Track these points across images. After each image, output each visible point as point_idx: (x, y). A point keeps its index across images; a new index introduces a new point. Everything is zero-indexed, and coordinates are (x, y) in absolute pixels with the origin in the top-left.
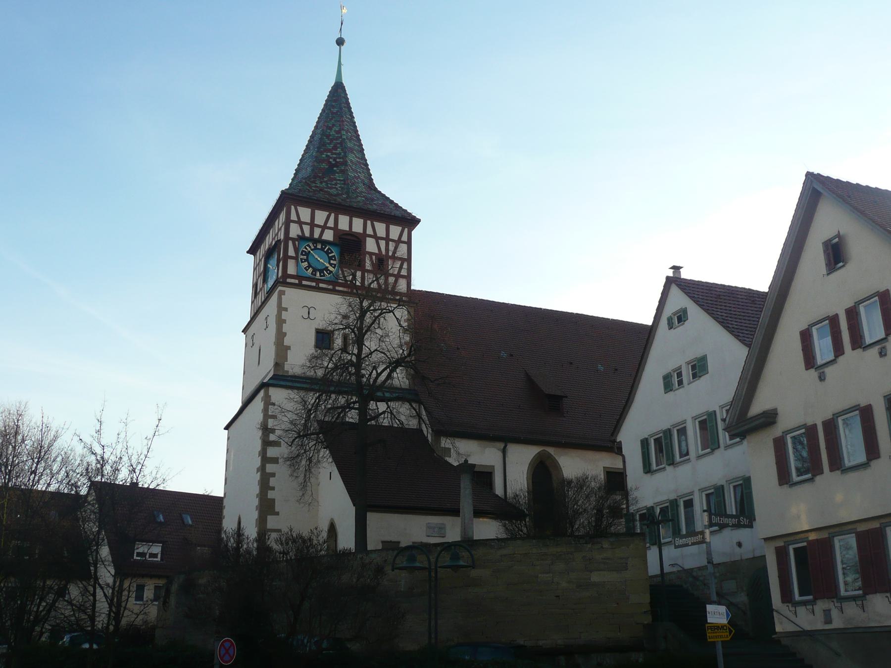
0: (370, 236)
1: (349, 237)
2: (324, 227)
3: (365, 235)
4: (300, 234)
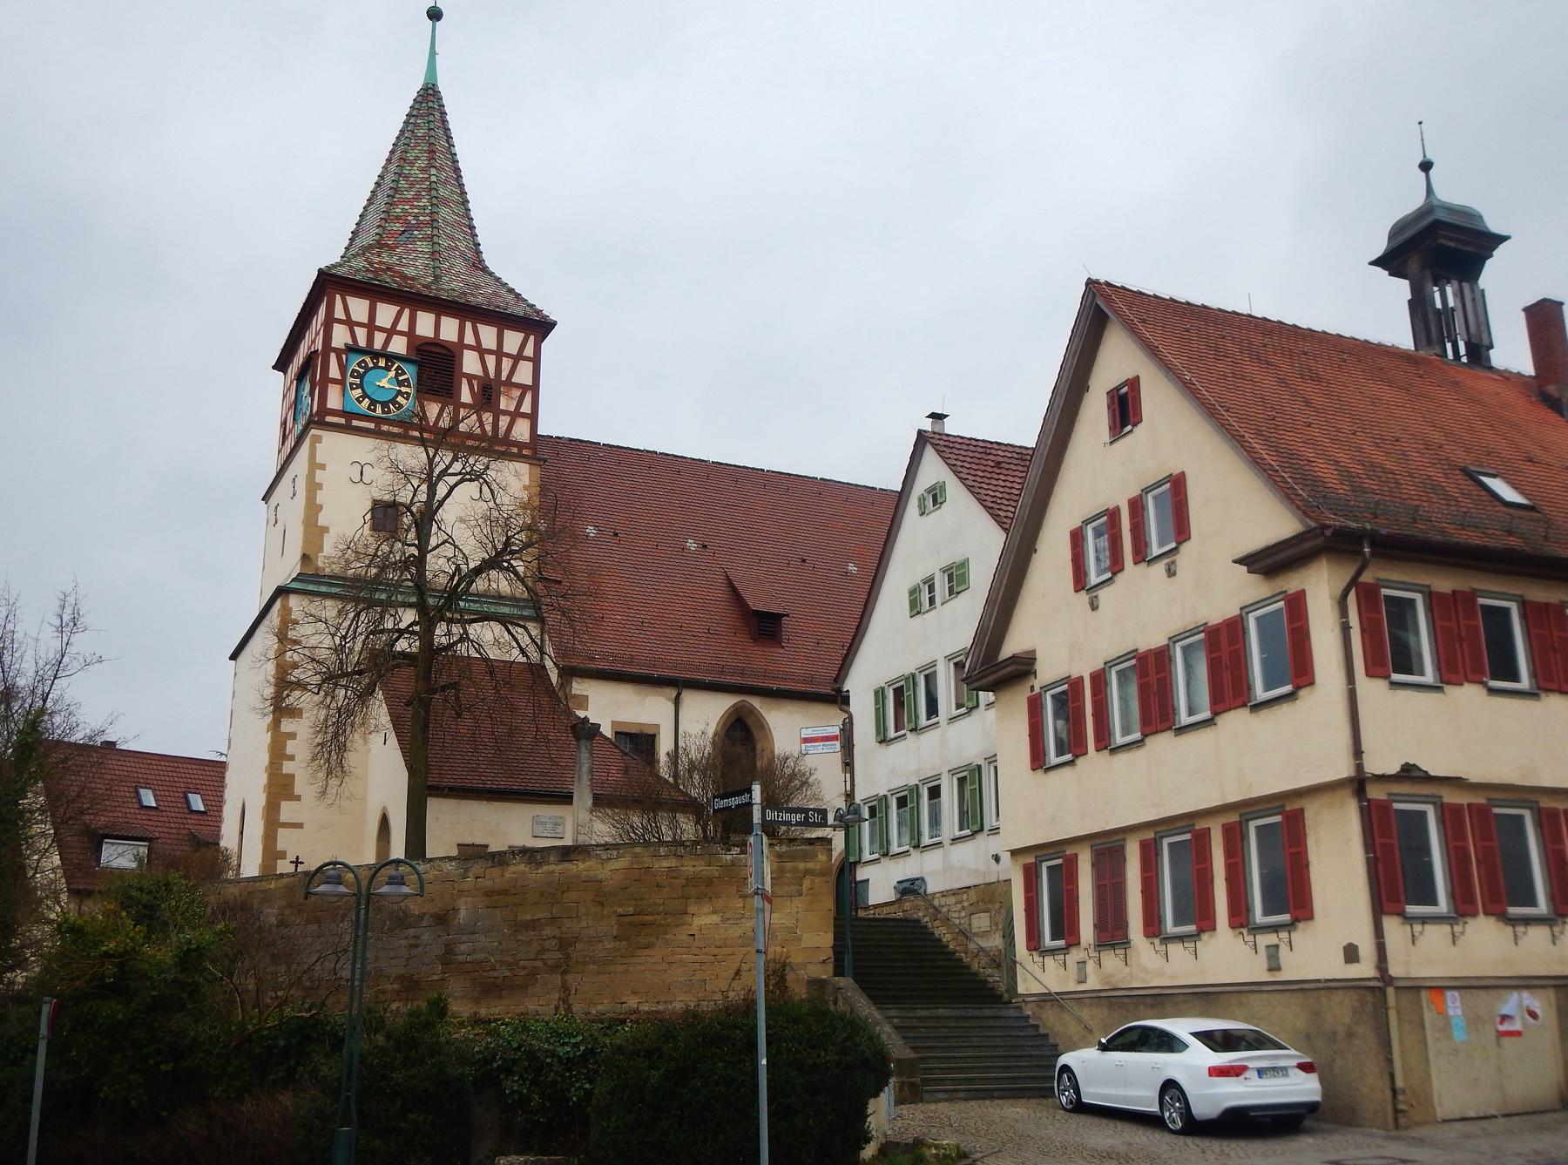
0: (470, 347)
1: (436, 350)
2: (391, 332)
3: (461, 345)
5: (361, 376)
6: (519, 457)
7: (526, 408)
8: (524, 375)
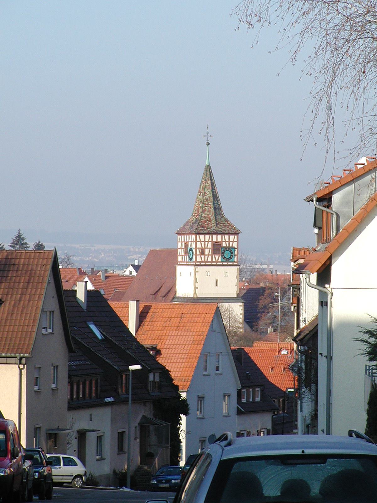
0: (224, 241)
3: (222, 241)
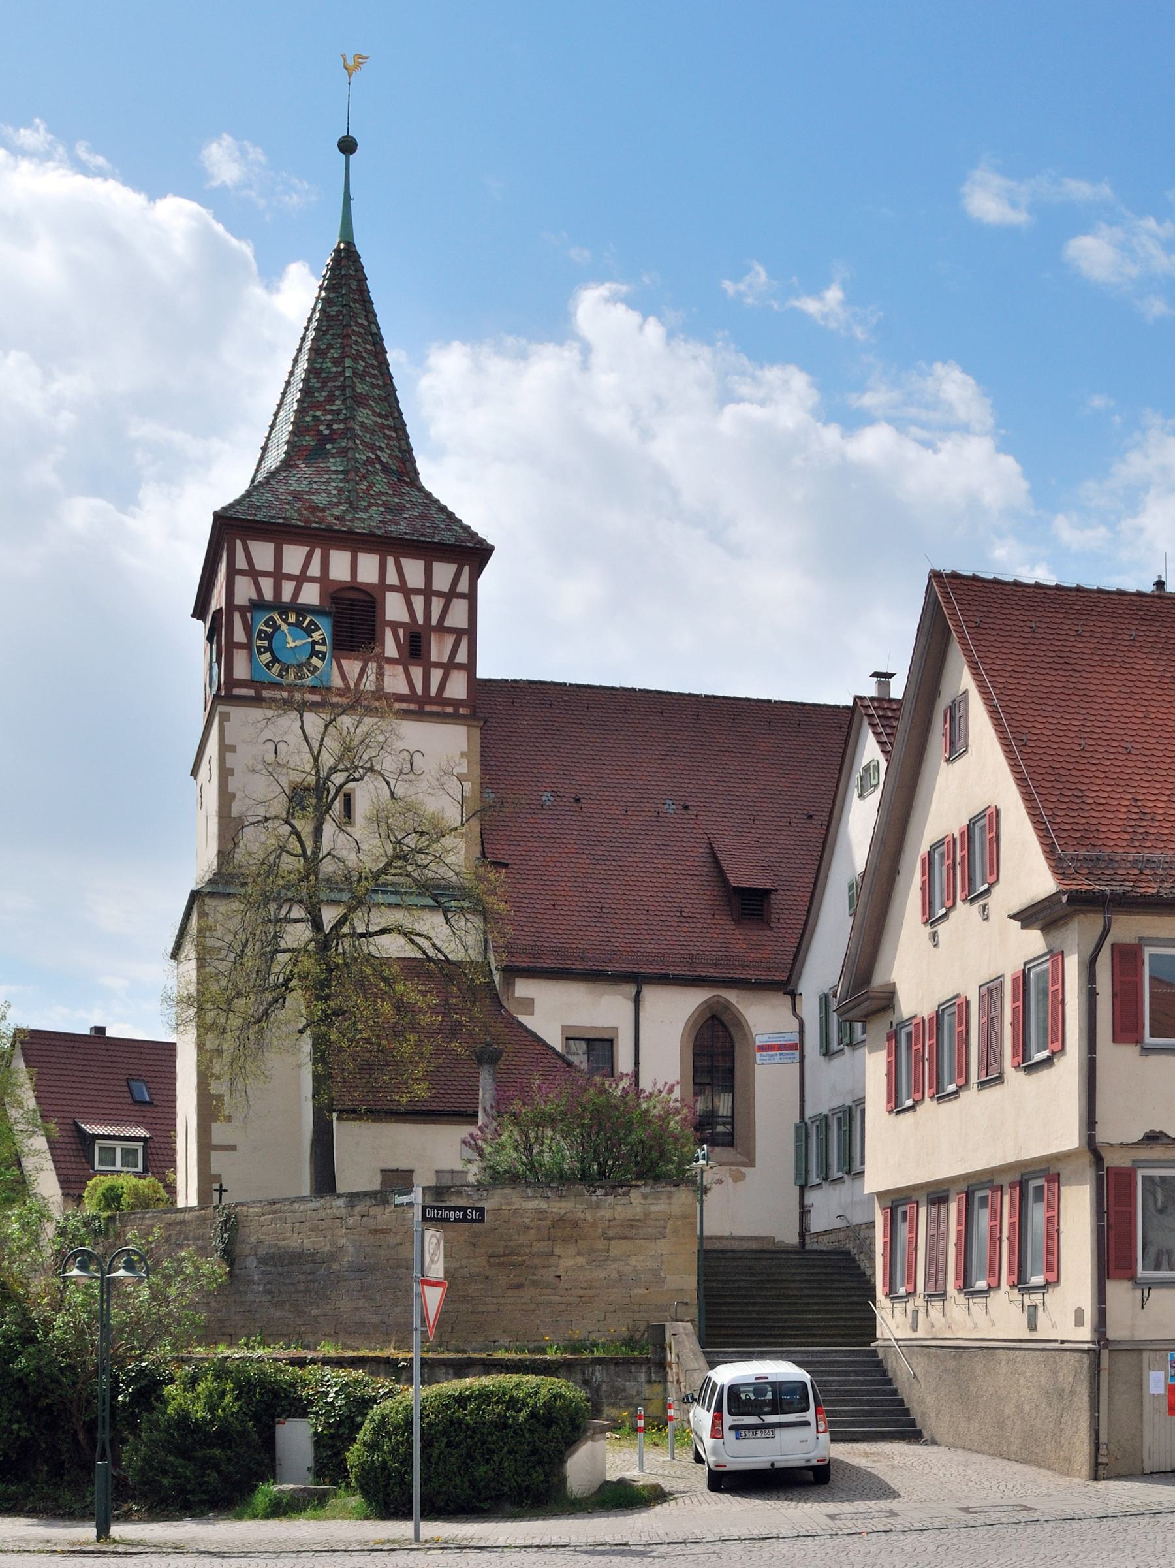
0: (393, 588)
2: (301, 579)
3: (383, 586)
4: (254, 596)
5: (269, 637)
6: (454, 718)
7: (462, 657)
8: (457, 617)
